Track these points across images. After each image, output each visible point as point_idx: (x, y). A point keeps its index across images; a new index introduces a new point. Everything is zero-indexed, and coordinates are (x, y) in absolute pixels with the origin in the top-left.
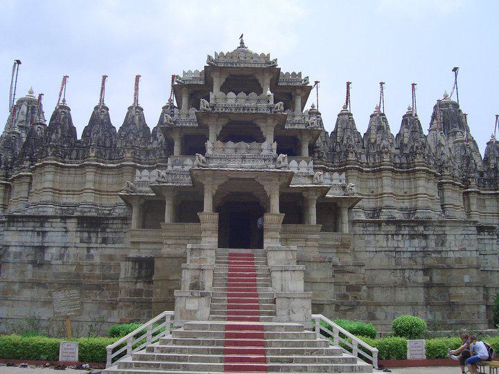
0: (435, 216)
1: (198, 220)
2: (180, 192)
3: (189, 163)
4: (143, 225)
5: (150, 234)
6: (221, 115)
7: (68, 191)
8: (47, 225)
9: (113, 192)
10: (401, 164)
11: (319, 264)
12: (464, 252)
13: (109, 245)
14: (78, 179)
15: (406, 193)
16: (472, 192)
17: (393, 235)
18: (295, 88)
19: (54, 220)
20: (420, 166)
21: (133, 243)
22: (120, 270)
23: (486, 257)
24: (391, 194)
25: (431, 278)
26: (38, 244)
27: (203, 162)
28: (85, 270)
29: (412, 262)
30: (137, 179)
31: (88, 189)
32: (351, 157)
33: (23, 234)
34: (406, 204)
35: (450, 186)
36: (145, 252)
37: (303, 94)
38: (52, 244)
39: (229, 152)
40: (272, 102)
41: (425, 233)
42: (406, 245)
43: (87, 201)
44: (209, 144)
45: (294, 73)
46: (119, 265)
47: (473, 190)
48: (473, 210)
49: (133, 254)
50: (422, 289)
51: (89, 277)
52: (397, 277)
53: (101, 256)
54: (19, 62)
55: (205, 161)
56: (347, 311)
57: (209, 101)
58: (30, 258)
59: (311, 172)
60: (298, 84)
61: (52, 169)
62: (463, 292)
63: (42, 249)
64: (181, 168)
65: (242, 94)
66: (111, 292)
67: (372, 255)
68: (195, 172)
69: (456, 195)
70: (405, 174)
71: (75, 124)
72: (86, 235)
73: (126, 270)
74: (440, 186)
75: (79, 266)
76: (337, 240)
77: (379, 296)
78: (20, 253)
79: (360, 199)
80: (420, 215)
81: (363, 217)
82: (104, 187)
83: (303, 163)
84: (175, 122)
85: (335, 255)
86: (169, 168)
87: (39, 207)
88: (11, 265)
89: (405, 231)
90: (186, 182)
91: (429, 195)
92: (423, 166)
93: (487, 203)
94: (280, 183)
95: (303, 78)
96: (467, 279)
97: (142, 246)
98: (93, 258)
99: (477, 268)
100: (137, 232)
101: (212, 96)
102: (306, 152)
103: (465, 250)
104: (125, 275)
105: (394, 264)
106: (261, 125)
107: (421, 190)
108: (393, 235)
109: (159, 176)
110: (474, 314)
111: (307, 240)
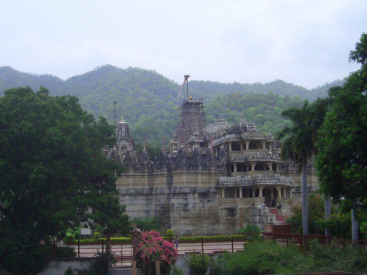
32: (290, 168)
36: (228, 206)
58: (182, 208)
63: (186, 205)
78: (178, 207)
107: (313, 180)
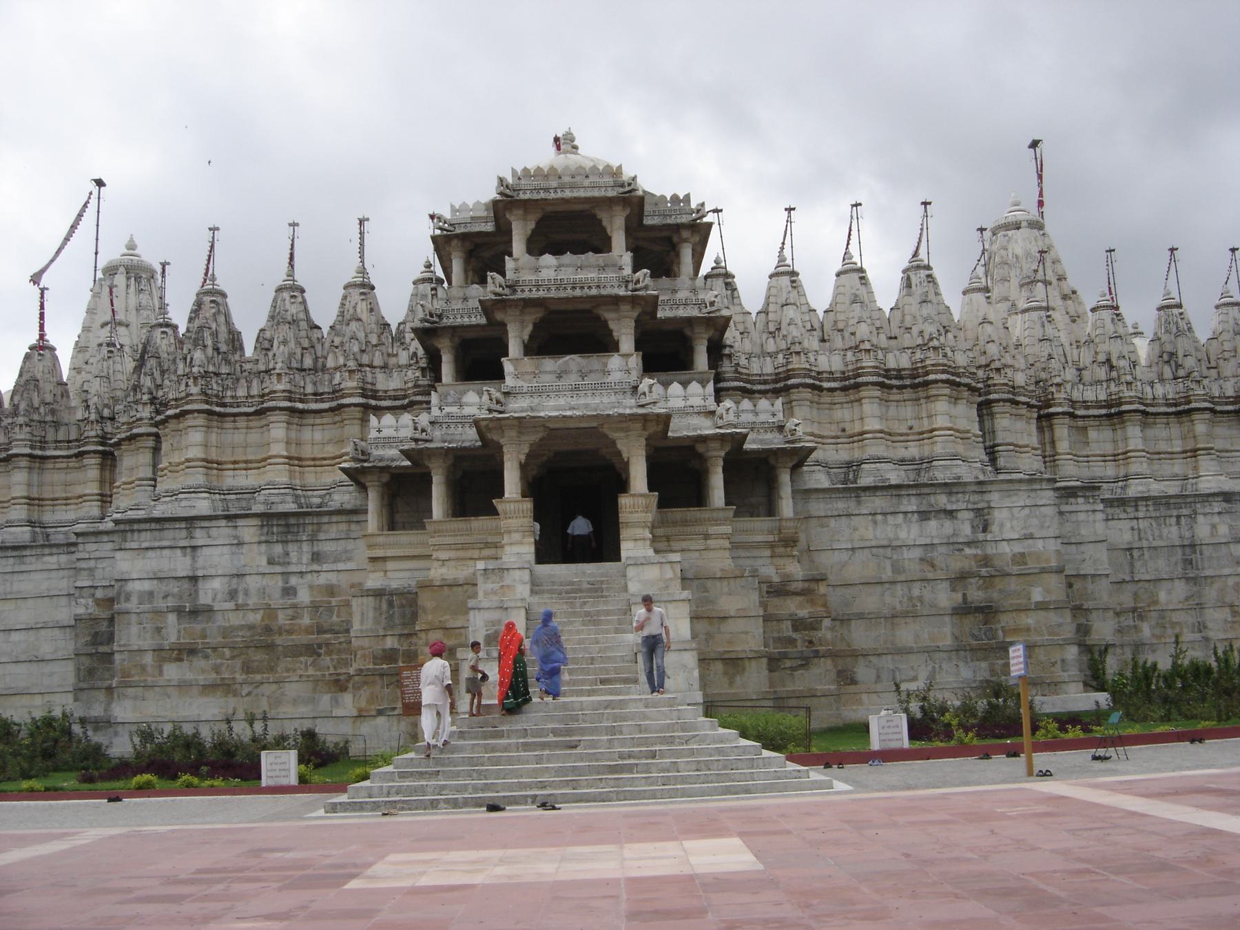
0: (967, 473)
1: (493, 512)
2: (458, 459)
3: (475, 401)
4: (392, 525)
6: (528, 303)
7: (235, 462)
8: (198, 533)
9: (325, 459)
10: (899, 370)
11: (732, 581)
12: (1030, 541)
13: (325, 567)
14: (254, 437)
15: (911, 428)
16: (1058, 414)
17: (884, 514)
18: (678, 227)
19: (214, 523)
20: (936, 372)
21: (373, 560)
22: (351, 614)
23: (1082, 548)
24: (881, 432)
25: (964, 595)
26: (184, 574)
27: (498, 402)
28: (282, 619)
29: (926, 567)
30: (373, 434)
31: (275, 457)
33: (150, 554)
34: (913, 451)
35: (1007, 407)
37: (697, 238)
38: (213, 572)
39: (548, 379)
40: (628, 270)
41: (949, 507)
42: (911, 533)
43: (272, 483)
44: (508, 367)
45: (675, 198)
46: (347, 604)
47: (1060, 410)
48: (1060, 451)
49: (374, 581)
50: (947, 619)
51: (290, 632)
52: (895, 598)
53: (311, 587)
54: (100, 183)
55: (502, 400)
56: (793, 669)
57: (503, 274)
58: (171, 602)
59: (711, 404)
60: (684, 219)
61: (200, 420)
62: (1030, 621)
64: (461, 409)
65: (568, 258)
66: (335, 657)
67: (844, 556)
68: (483, 424)
69: (1020, 425)
70: (909, 390)
71: (239, 325)
72: (278, 549)
73: (363, 619)
74: (985, 409)
75: (270, 611)
76: (770, 532)
77: (861, 636)
78: (151, 594)
79: (815, 448)
80: (941, 476)
81: (825, 484)
82: (307, 452)
83: (694, 387)
84: (440, 316)
85: (769, 560)
86: (435, 411)
87: (181, 500)
88: (134, 618)
89: (911, 504)
90: (469, 437)
91: (958, 431)
92: (943, 372)
93: (1093, 434)
94: (646, 433)
95: (693, 205)
96: (1037, 595)
97: (390, 565)
98: (295, 594)
99: (1060, 571)
100: (381, 540)
101: (509, 264)
102: (701, 360)
103: (1031, 537)
104: (362, 622)
105: (890, 573)
106: (609, 315)
108: (884, 514)
109: (416, 429)
110: (1054, 664)
111: (707, 537)
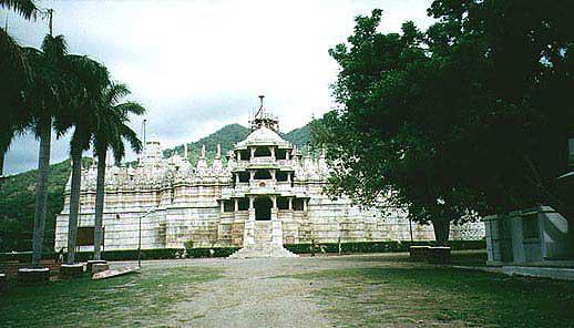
5: (229, 214)
36: (227, 221)
